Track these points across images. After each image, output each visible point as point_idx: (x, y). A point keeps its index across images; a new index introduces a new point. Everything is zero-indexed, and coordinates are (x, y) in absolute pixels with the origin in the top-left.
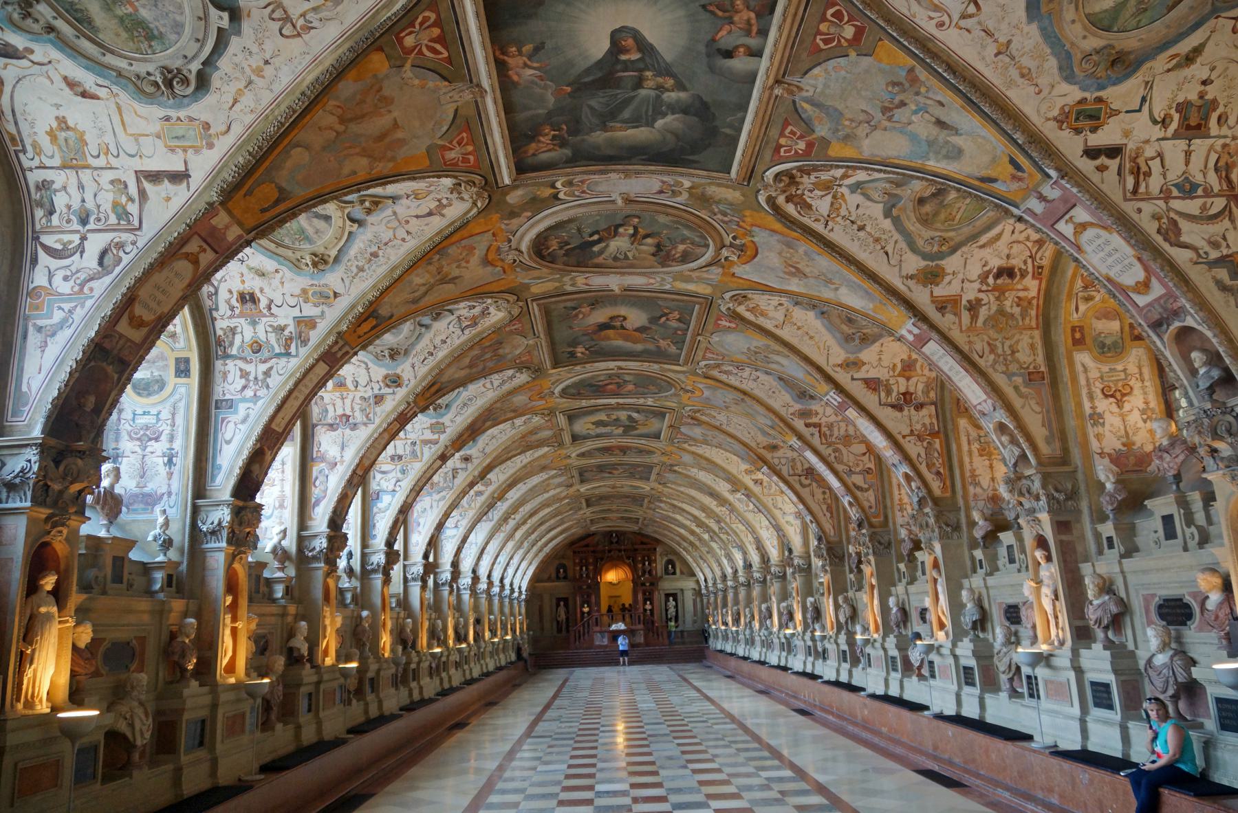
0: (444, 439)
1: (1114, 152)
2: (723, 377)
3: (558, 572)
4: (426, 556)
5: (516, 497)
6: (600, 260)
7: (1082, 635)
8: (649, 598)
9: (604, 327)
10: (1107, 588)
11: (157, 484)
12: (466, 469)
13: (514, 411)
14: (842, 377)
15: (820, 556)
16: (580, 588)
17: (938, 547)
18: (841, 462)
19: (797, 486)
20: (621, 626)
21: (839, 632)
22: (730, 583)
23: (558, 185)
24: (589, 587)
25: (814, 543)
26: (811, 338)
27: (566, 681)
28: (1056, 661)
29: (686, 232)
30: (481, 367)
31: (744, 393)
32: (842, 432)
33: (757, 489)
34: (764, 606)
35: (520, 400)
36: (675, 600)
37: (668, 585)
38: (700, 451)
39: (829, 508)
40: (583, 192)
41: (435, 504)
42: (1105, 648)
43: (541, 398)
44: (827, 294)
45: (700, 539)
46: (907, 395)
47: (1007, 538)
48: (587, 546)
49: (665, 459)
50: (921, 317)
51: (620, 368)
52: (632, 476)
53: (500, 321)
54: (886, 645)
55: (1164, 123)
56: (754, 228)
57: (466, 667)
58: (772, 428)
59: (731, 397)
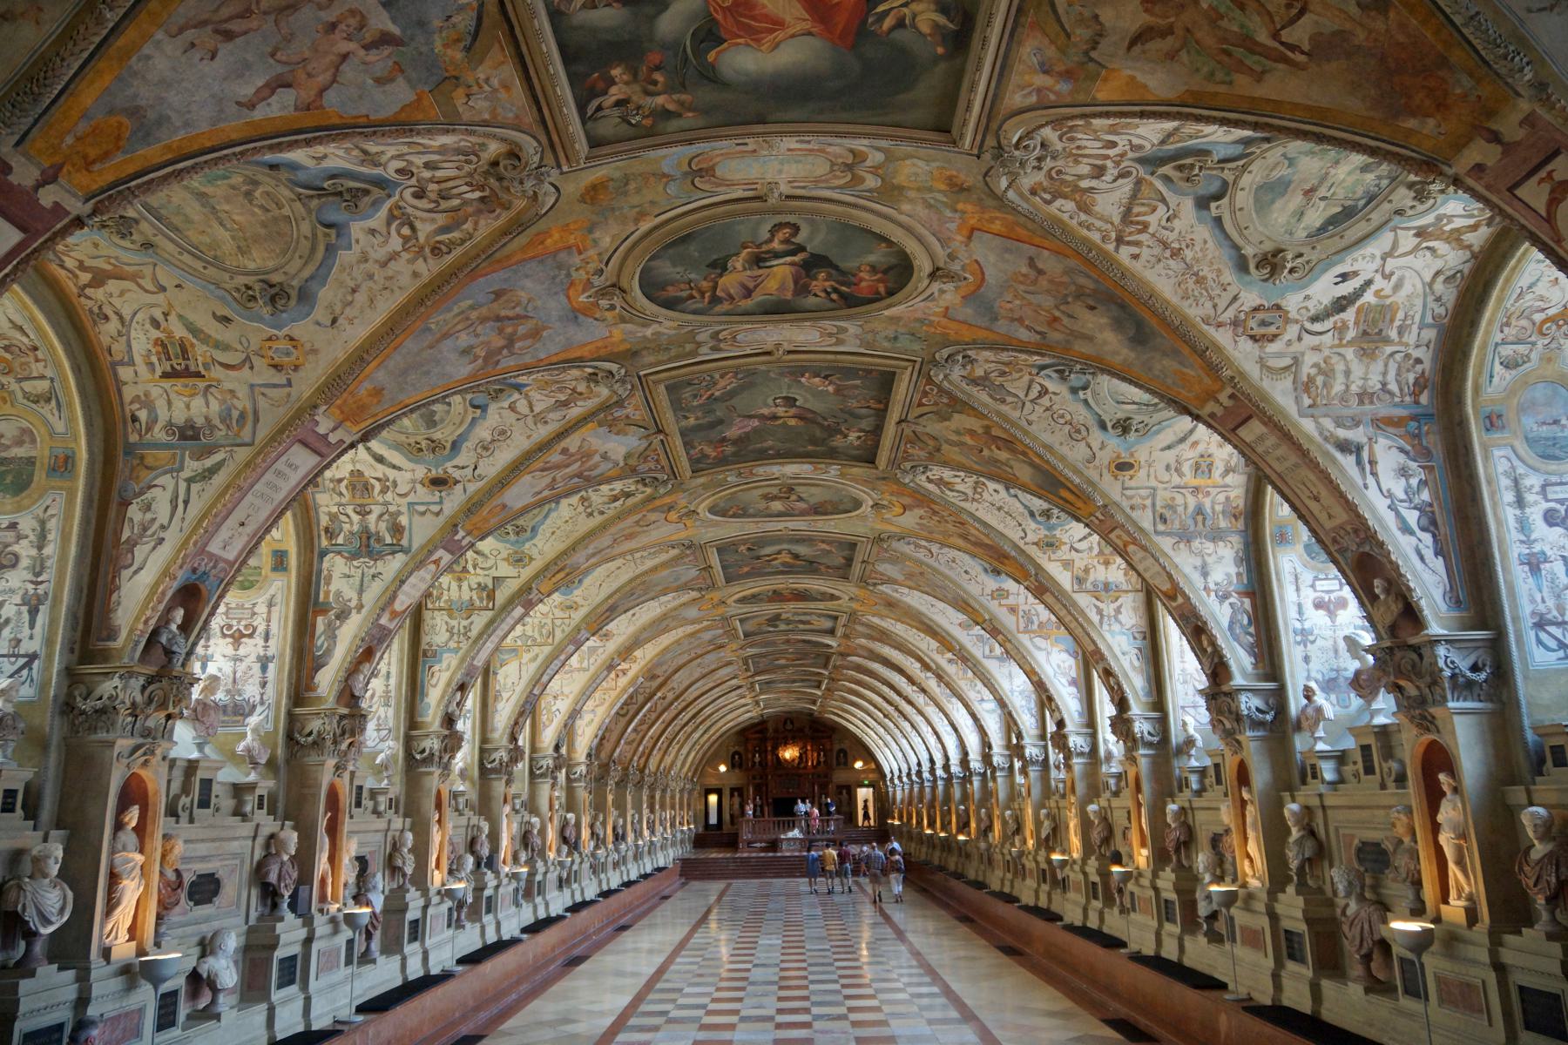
4: (557, 748)
7: (1278, 878)
11: (251, 691)
42: (1298, 893)
54: (1088, 869)
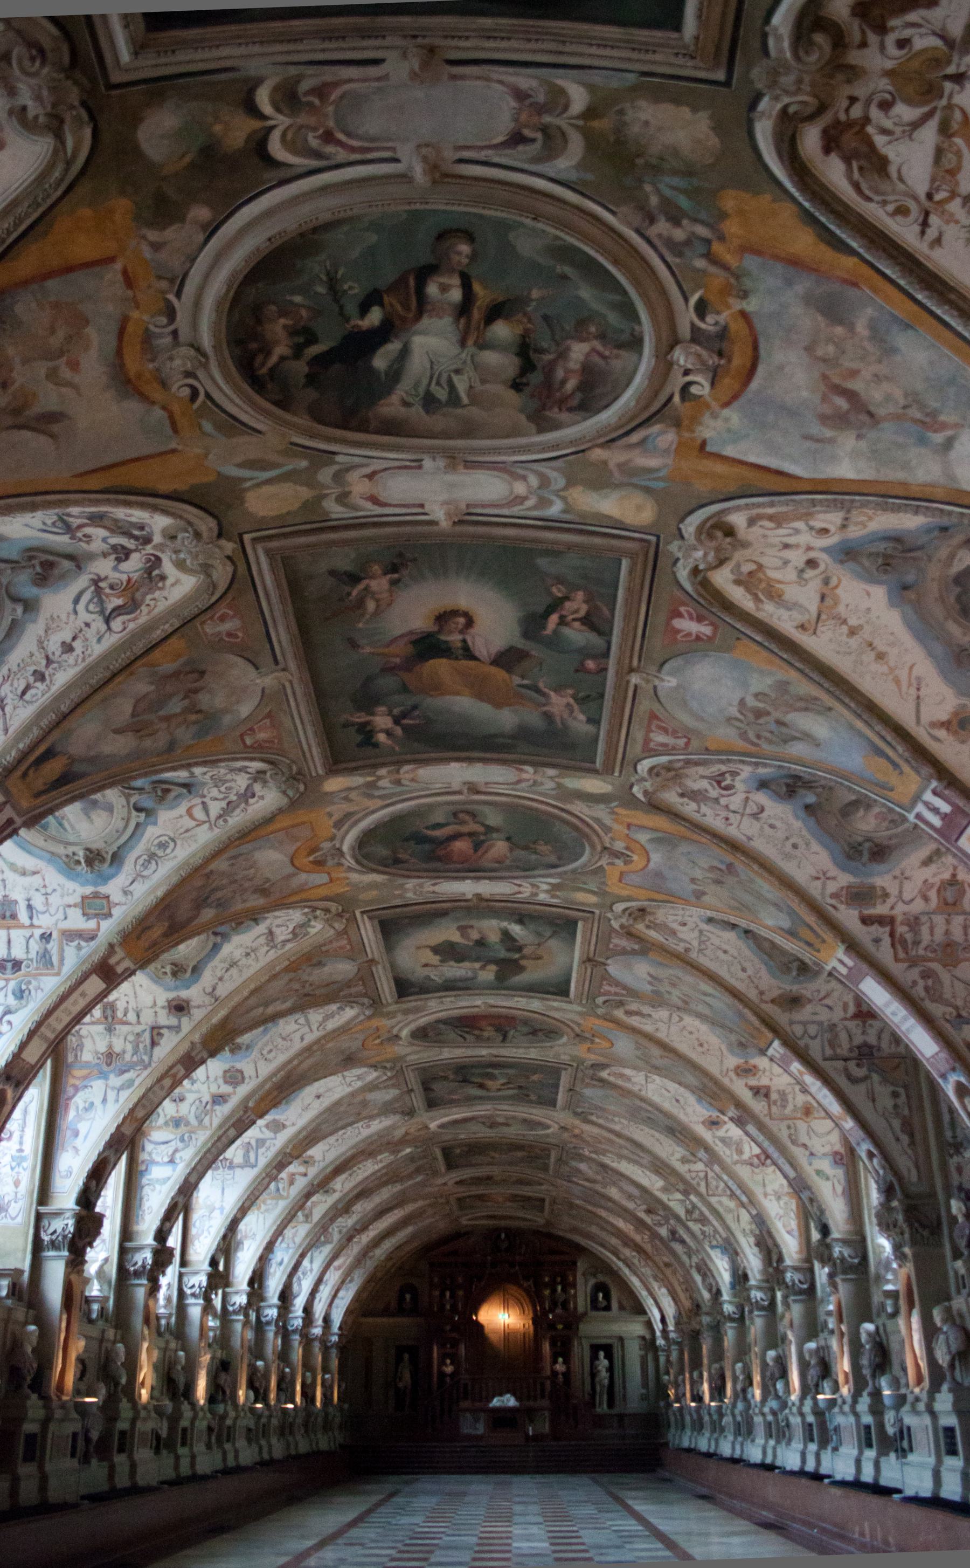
0: (107, 928)
2: (689, 808)
3: (401, 1299)
5: (301, 1123)
6: (391, 407)
8: (563, 1349)
9: (428, 646)
12: (177, 1029)
13: (263, 891)
18: (939, 999)
19: (842, 1082)
20: (510, 1401)
21: (935, 1388)
23: (263, 99)
26: (881, 656)
27: (392, 1495)
29: (586, 293)
30: (162, 740)
31: (733, 846)
32: (939, 936)
33: (758, 1107)
34: (771, 1354)
35: (271, 859)
36: (609, 1356)
37: (599, 1327)
38: (648, 1028)
39: (907, 1126)
40: (328, 137)
41: (111, 1095)
43: (319, 863)
49: (581, 1051)
51: (473, 788)
52: (523, 1095)
53: (187, 600)
56: (751, 262)
57: (182, 1451)
58: (792, 933)
59: (705, 862)
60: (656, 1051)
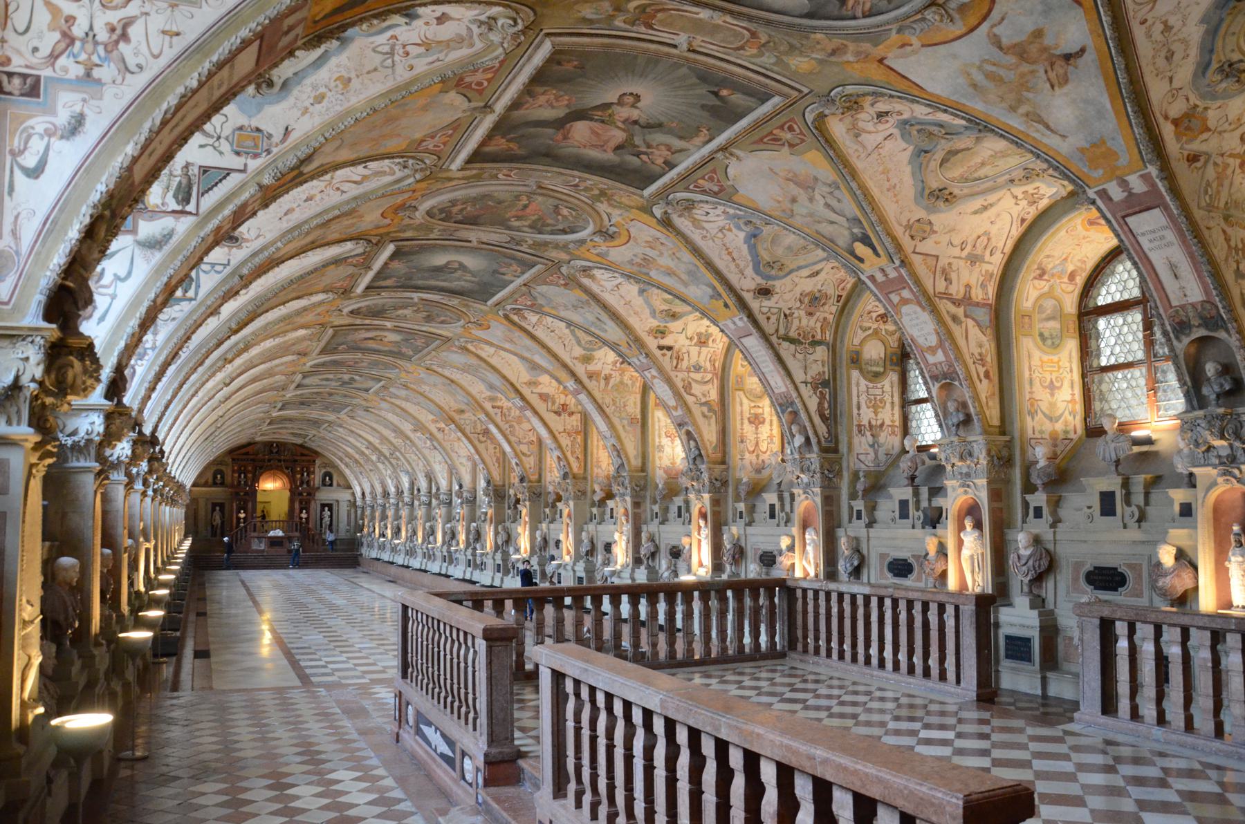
1: (670, 348)
2: (440, 370)
3: (215, 477)
7: (637, 561)
8: (305, 506)
10: (652, 539)
14: (526, 391)
15: (487, 495)
16: (237, 494)
17: (571, 503)
19: (476, 442)
20: (279, 533)
21: (496, 551)
22: (392, 501)
24: (246, 493)
25: (482, 484)
28: (623, 575)
33: (439, 435)
34: (428, 524)
37: (325, 495)
39: (498, 460)
44: (527, 355)
45: (368, 459)
46: (564, 407)
47: (610, 503)
48: (247, 454)
50: (578, 380)
55: (691, 339)
60: (398, 410)
